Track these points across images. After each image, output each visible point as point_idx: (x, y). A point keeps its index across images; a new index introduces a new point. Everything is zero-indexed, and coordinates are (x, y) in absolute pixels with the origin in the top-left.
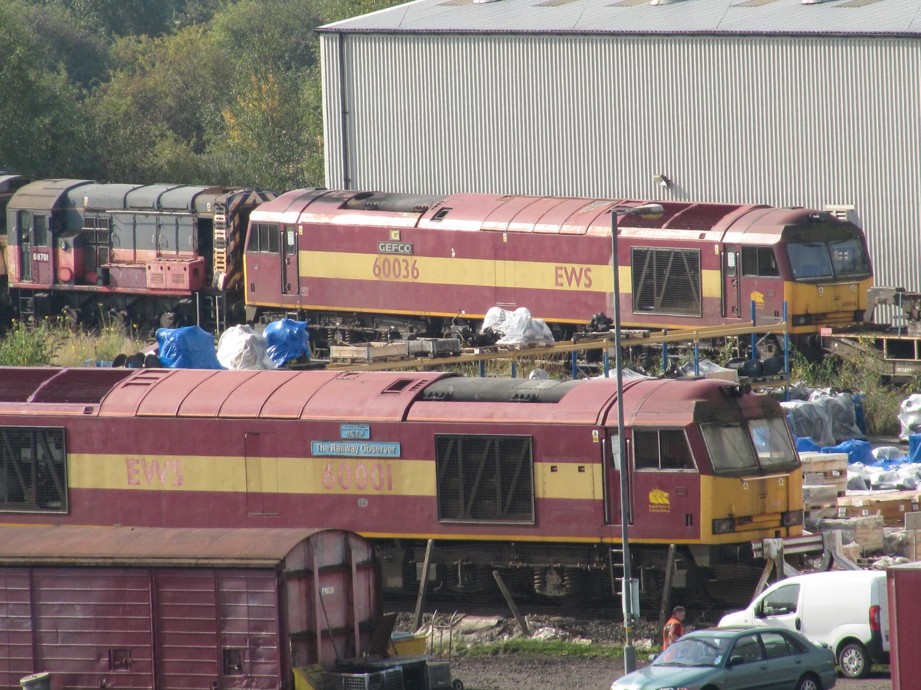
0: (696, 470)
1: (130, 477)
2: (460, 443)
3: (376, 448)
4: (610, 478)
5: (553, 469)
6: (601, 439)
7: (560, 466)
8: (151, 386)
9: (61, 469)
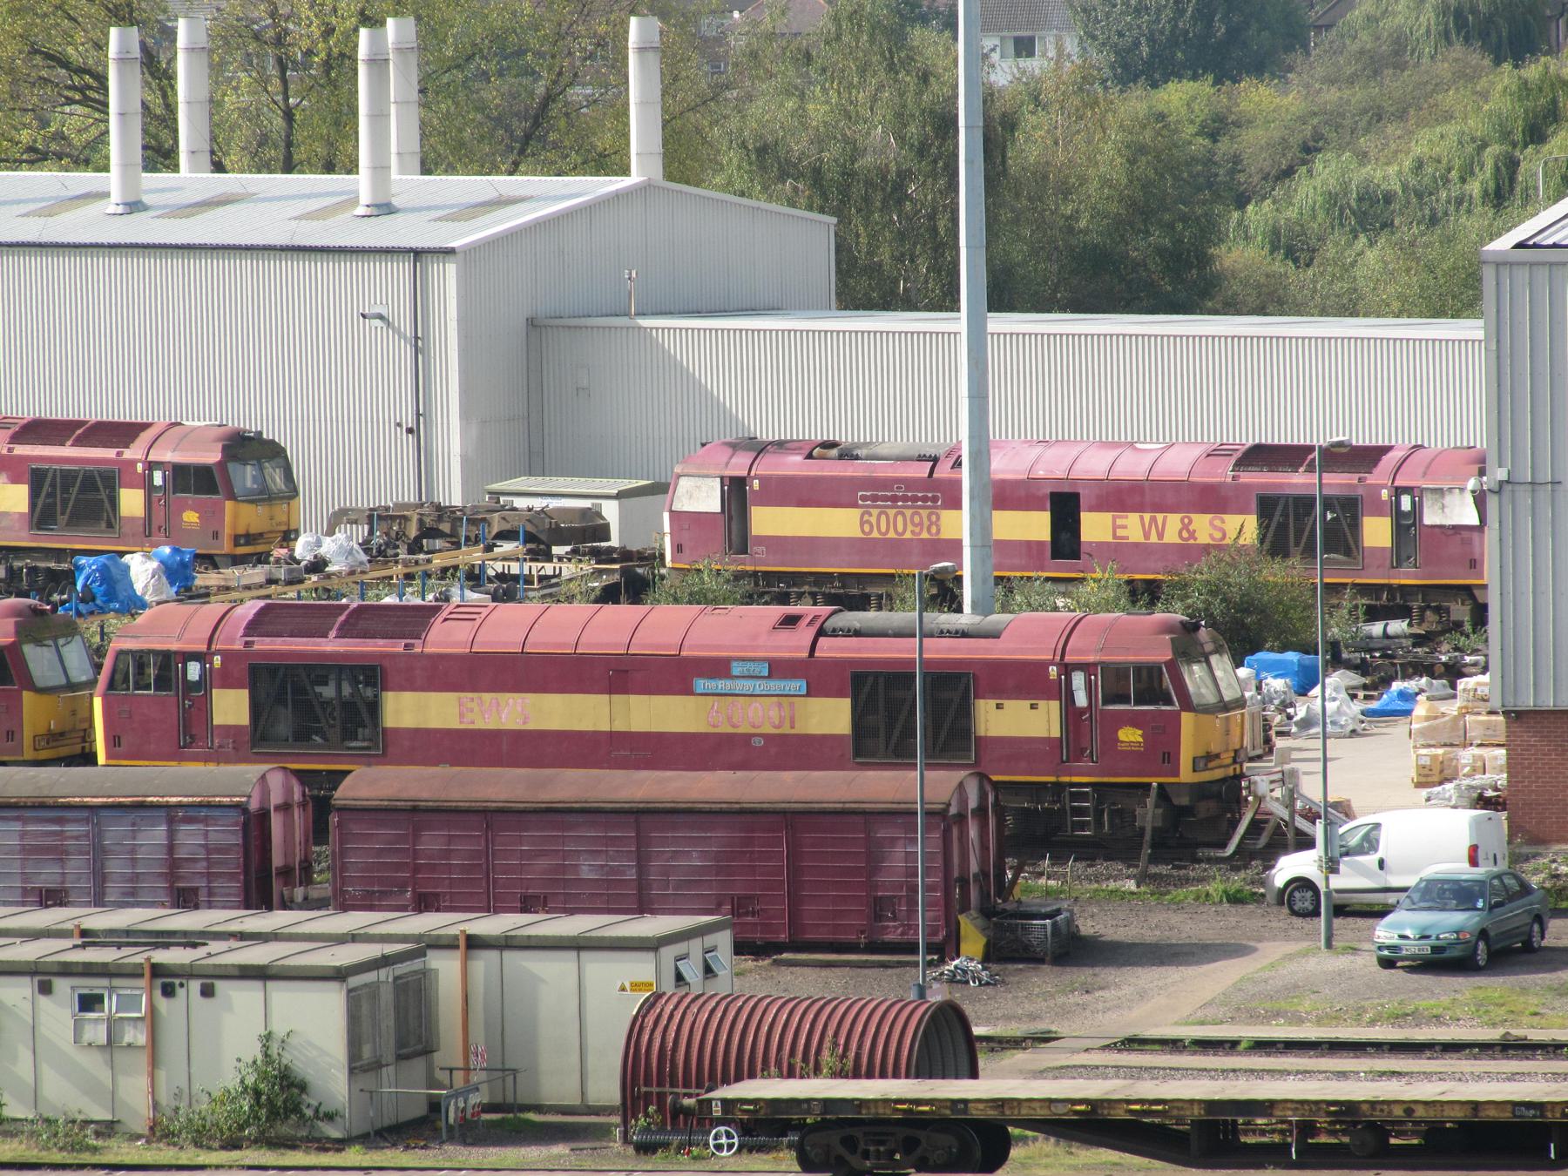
0: (1177, 707)
1: (462, 715)
2: (881, 681)
3: (776, 685)
4: (1071, 714)
5: (999, 707)
6: (1059, 675)
7: (1007, 703)
8: (479, 621)
9: (374, 708)
